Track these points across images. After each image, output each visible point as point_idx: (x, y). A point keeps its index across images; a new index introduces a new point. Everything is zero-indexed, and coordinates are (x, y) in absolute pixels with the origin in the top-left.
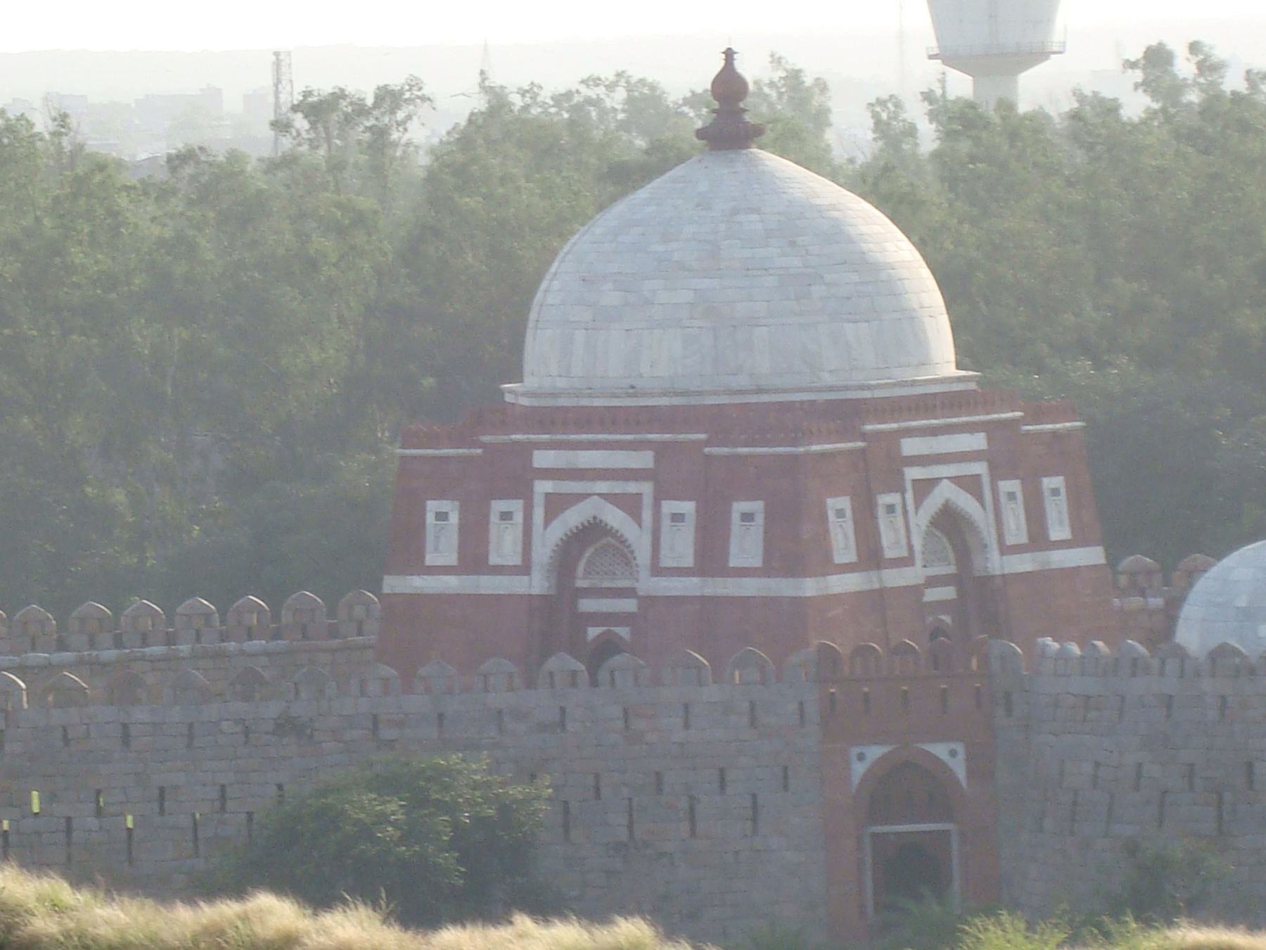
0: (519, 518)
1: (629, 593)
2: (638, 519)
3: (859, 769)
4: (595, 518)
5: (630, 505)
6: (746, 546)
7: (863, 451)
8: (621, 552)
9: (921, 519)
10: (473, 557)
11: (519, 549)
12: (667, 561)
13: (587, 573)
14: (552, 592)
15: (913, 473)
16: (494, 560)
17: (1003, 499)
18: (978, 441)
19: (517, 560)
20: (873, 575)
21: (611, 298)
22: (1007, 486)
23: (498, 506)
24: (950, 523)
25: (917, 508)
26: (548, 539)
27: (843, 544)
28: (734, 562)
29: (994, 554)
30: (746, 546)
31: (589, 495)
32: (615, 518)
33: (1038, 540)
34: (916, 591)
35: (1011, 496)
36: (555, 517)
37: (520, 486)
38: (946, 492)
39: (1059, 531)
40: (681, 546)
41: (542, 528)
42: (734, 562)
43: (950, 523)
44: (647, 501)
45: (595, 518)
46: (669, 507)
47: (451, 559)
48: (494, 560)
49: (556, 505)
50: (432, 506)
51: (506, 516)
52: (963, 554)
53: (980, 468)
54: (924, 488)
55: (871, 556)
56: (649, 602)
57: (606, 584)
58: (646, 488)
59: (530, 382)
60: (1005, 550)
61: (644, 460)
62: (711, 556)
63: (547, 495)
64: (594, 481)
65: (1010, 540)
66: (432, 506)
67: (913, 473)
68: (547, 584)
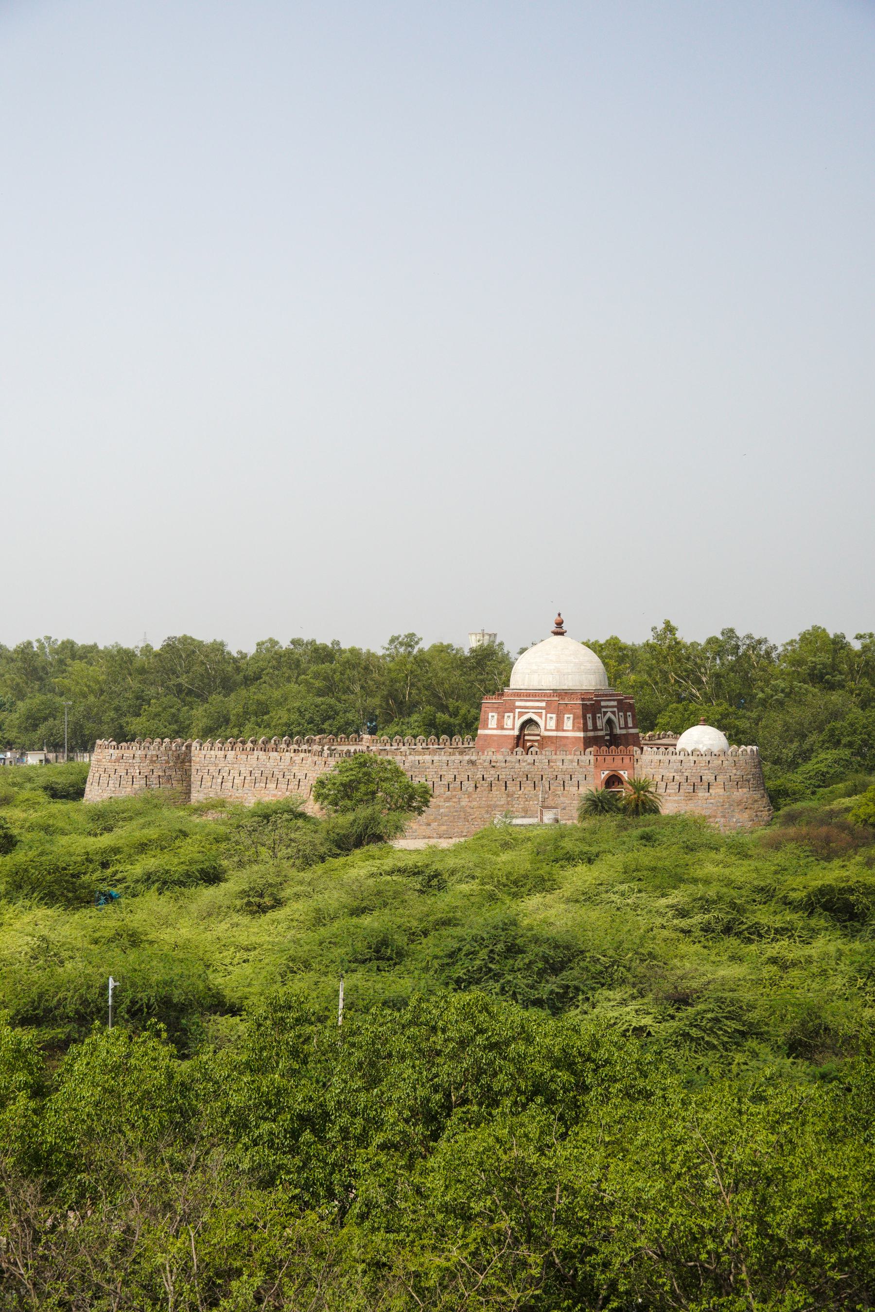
0: (512, 717)
1: (538, 735)
2: (541, 717)
3: (603, 776)
5: (540, 715)
8: (536, 724)
9: (605, 720)
10: (501, 727)
12: (548, 728)
15: (603, 710)
18: (615, 703)
21: (535, 667)
22: (621, 714)
23: (507, 715)
24: (610, 722)
32: (535, 718)
33: (626, 727)
34: (603, 737)
37: (512, 710)
38: (609, 714)
39: (630, 725)
43: (610, 722)
47: (495, 726)
49: (521, 714)
50: (490, 714)
52: (611, 729)
53: (615, 709)
54: (605, 713)
55: (595, 729)
56: (543, 738)
57: (532, 732)
58: (544, 711)
59: (512, 687)
60: (620, 728)
61: (543, 704)
62: (559, 727)
64: (532, 709)
66: (490, 714)
67: (603, 710)
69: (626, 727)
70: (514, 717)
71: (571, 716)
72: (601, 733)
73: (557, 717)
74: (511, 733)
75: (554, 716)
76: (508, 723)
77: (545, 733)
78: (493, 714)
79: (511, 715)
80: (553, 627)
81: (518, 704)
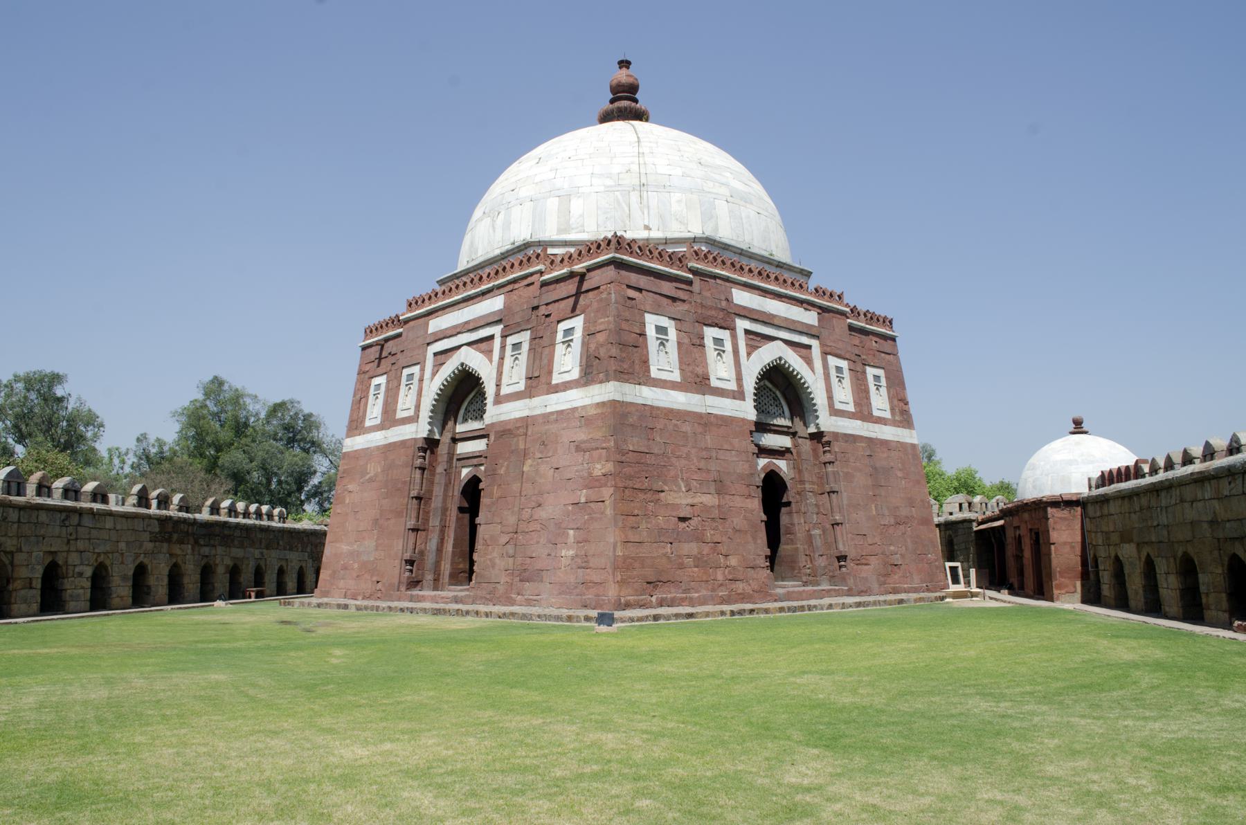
0: (416, 378)
4: (462, 364)
6: (567, 362)
9: (754, 366)
10: (389, 419)
12: (505, 390)
13: (465, 420)
16: (400, 414)
17: (833, 373)
19: (411, 413)
22: (833, 361)
23: (406, 372)
25: (749, 354)
26: (433, 387)
28: (556, 379)
30: (567, 362)
31: (459, 347)
33: (863, 412)
35: (839, 369)
44: (497, 342)
45: (462, 364)
46: (511, 340)
48: (400, 414)
54: (756, 339)
55: (698, 382)
58: (497, 330)
60: (835, 412)
61: (495, 304)
65: (838, 406)
67: (742, 324)
69: (863, 412)
70: (421, 380)
73: (533, 339)
75: (525, 337)
79: (416, 370)
80: (603, 101)
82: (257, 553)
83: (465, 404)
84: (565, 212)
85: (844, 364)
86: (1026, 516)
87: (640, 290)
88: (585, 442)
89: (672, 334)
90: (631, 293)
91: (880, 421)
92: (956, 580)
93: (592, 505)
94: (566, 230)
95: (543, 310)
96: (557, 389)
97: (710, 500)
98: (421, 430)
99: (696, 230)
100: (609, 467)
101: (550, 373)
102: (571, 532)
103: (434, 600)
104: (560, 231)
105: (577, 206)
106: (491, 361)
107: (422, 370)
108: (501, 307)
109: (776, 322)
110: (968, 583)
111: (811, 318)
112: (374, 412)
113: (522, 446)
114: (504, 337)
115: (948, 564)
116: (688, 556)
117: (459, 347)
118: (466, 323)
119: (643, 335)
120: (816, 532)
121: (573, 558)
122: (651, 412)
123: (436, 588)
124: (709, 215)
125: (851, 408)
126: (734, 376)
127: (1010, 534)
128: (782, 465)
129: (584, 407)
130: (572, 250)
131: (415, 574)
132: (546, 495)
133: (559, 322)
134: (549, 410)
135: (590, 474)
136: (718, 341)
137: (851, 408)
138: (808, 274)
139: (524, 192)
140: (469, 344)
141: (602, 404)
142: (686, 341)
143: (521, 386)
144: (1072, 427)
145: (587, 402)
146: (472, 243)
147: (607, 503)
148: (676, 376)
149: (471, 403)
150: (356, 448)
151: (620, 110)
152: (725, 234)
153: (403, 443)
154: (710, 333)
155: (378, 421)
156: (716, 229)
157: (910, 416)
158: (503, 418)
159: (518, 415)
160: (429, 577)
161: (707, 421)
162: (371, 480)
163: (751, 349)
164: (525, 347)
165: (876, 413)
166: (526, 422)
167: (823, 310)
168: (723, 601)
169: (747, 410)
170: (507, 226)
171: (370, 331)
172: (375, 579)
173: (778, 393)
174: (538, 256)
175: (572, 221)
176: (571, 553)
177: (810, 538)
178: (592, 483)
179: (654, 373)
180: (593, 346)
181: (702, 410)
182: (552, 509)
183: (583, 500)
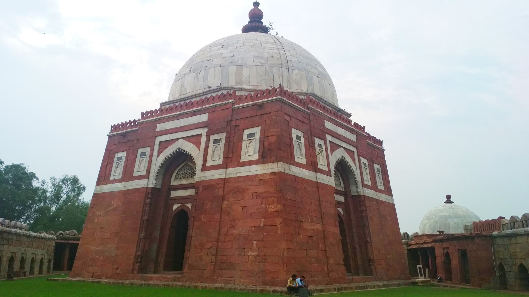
5: (195, 140)
6: (250, 150)
7: (309, 114)
10: (128, 175)
11: (146, 168)
12: (209, 163)
13: (176, 178)
14: (159, 187)
16: (136, 174)
19: (144, 173)
20: (313, 173)
22: (363, 160)
26: (159, 161)
27: (300, 157)
28: (243, 159)
29: (360, 185)
30: (250, 150)
32: (189, 148)
35: (365, 164)
36: (162, 152)
40: (216, 156)
41: (156, 157)
42: (243, 159)
43: (342, 169)
45: (179, 149)
46: (213, 137)
48: (136, 174)
51: (143, 154)
52: (347, 186)
54: (334, 147)
55: (313, 166)
58: (203, 132)
60: (364, 185)
61: (204, 118)
63: (160, 142)
65: (366, 183)
67: (329, 138)
68: (155, 182)
69: (374, 187)
70: (151, 156)
71: (257, 131)
72: (323, 179)
74: (142, 184)
75: (223, 136)
76: (140, 168)
77: (200, 176)
78: (120, 155)
79: (148, 150)
80: (246, 21)
81: (160, 127)
82: (23, 249)
83: (177, 170)
84: (239, 74)
85: (366, 161)
86: (455, 242)
87: (290, 116)
88: (262, 193)
89: (302, 139)
90: (287, 118)
91: (380, 191)
92: (421, 276)
93: (268, 228)
94: (241, 83)
95: (233, 123)
96: (244, 164)
97: (319, 227)
98: (151, 183)
99: (304, 89)
100: (279, 207)
101: (240, 156)
102: (255, 242)
103: (158, 279)
104: (237, 83)
105: (246, 72)
106: (199, 148)
107: (152, 151)
108: (207, 120)
109: (341, 138)
110: (425, 276)
111: (353, 137)
112: (117, 172)
113: (221, 193)
114: (208, 136)
115: (418, 266)
116: (314, 258)
117: (178, 139)
118: (184, 127)
119: (291, 139)
120: (357, 247)
121: (255, 257)
122: (296, 179)
123: (155, 273)
124: (310, 83)
125: (369, 184)
126: (326, 164)
127: (439, 252)
128: (341, 210)
129: (262, 175)
130: (253, 93)
131: (143, 264)
132: (237, 221)
133: (244, 129)
134: (238, 175)
135: (266, 211)
136: (320, 146)
137: (369, 184)
138: (350, 115)
139: (216, 62)
140: (184, 138)
141: (274, 174)
142: (308, 144)
143: (220, 162)
144: (445, 200)
145: (264, 172)
146: (182, 87)
147: (279, 226)
148: (303, 161)
149: (181, 169)
150: (103, 191)
151: (255, 27)
152: (318, 93)
153: (138, 190)
154: (317, 141)
155: (120, 177)
156: (313, 89)
157: (391, 190)
158: (208, 178)
159: (218, 177)
160: (152, 266)
161: (318, 185)
162: (114, 209)
163: (332, 151)
164: (223, 142)
165: (379, 187)
166: (225, 181)
167: (358, 135)
168: (329, 283)
169: (330, 181)
170: (206, 78)
171: (114, 128)
172: (115, 266)
173: (339, 174)
174: (230, 95)
175: (244, 79)
176: (255, 254)
177: (354, 248)
178: (266, 215)
179: (297, 160)
180: (266, 143)
181: (314, 180)
182: (242, 228)
183: (262, 225)
